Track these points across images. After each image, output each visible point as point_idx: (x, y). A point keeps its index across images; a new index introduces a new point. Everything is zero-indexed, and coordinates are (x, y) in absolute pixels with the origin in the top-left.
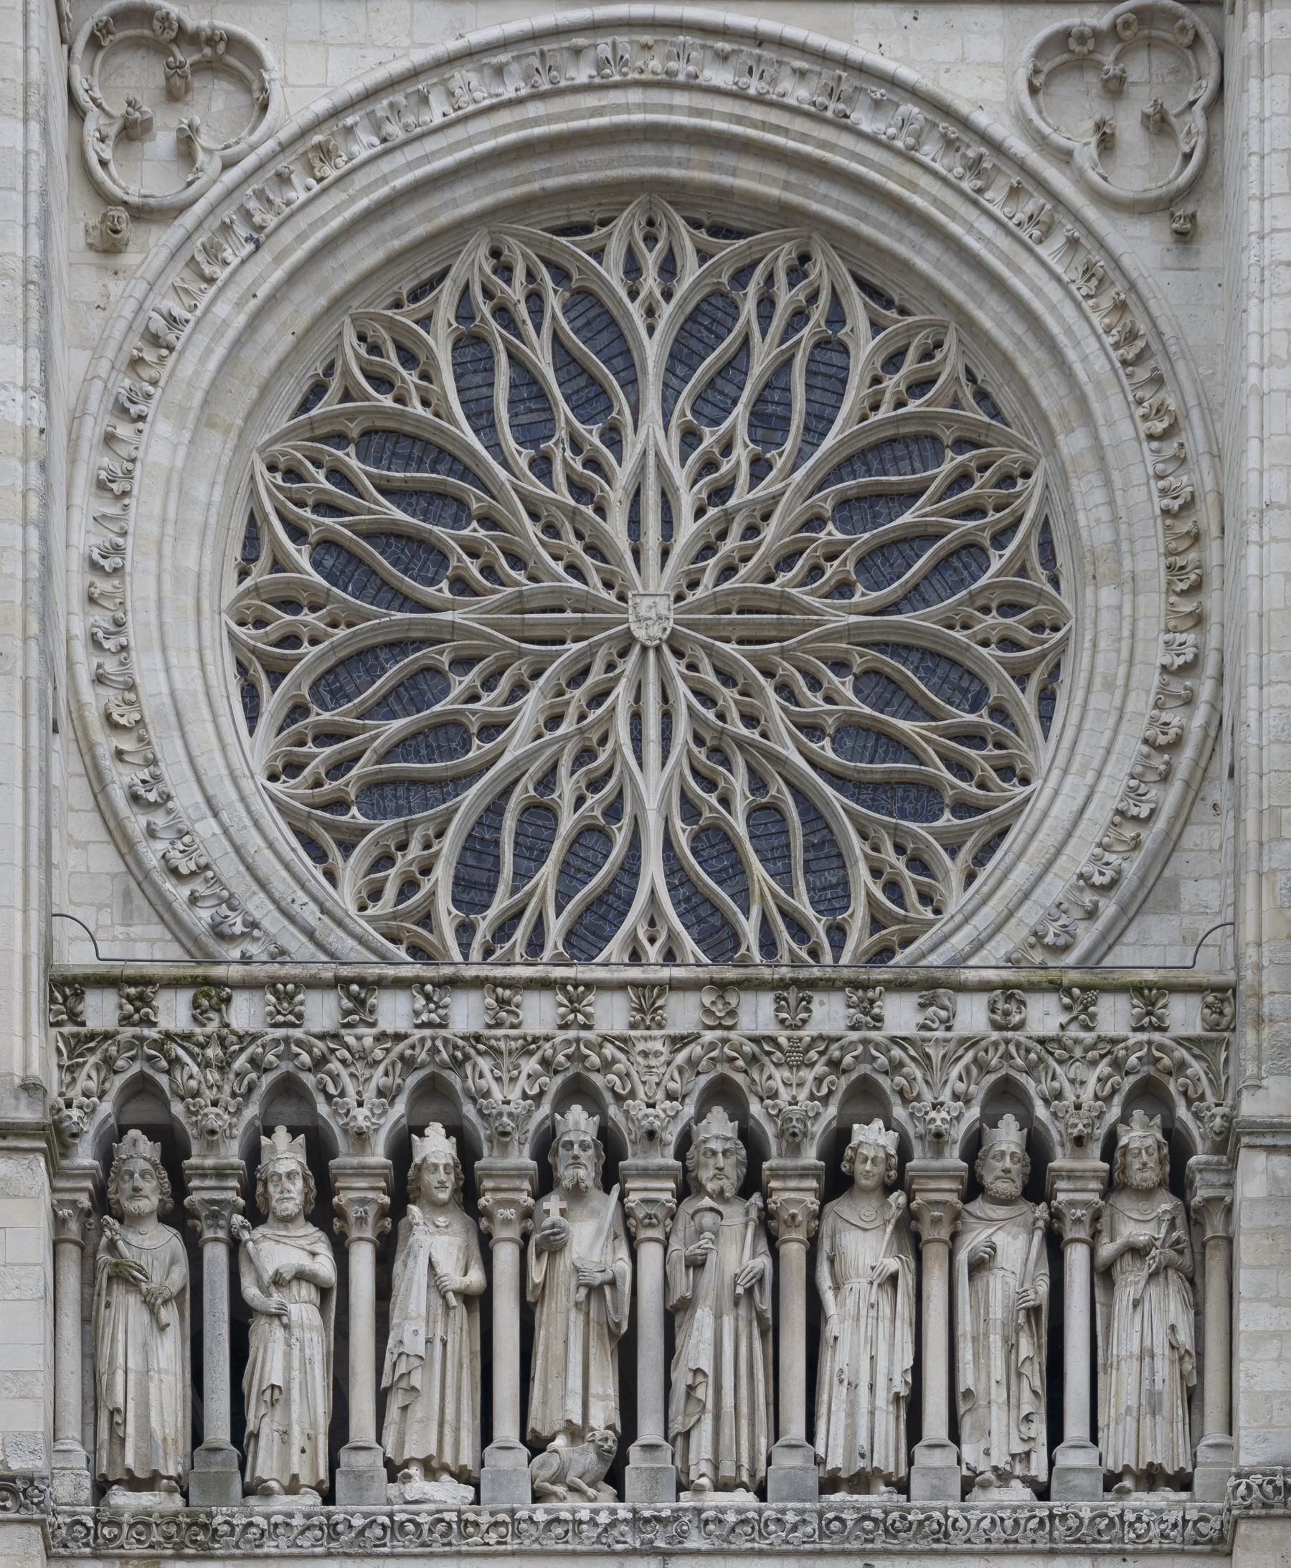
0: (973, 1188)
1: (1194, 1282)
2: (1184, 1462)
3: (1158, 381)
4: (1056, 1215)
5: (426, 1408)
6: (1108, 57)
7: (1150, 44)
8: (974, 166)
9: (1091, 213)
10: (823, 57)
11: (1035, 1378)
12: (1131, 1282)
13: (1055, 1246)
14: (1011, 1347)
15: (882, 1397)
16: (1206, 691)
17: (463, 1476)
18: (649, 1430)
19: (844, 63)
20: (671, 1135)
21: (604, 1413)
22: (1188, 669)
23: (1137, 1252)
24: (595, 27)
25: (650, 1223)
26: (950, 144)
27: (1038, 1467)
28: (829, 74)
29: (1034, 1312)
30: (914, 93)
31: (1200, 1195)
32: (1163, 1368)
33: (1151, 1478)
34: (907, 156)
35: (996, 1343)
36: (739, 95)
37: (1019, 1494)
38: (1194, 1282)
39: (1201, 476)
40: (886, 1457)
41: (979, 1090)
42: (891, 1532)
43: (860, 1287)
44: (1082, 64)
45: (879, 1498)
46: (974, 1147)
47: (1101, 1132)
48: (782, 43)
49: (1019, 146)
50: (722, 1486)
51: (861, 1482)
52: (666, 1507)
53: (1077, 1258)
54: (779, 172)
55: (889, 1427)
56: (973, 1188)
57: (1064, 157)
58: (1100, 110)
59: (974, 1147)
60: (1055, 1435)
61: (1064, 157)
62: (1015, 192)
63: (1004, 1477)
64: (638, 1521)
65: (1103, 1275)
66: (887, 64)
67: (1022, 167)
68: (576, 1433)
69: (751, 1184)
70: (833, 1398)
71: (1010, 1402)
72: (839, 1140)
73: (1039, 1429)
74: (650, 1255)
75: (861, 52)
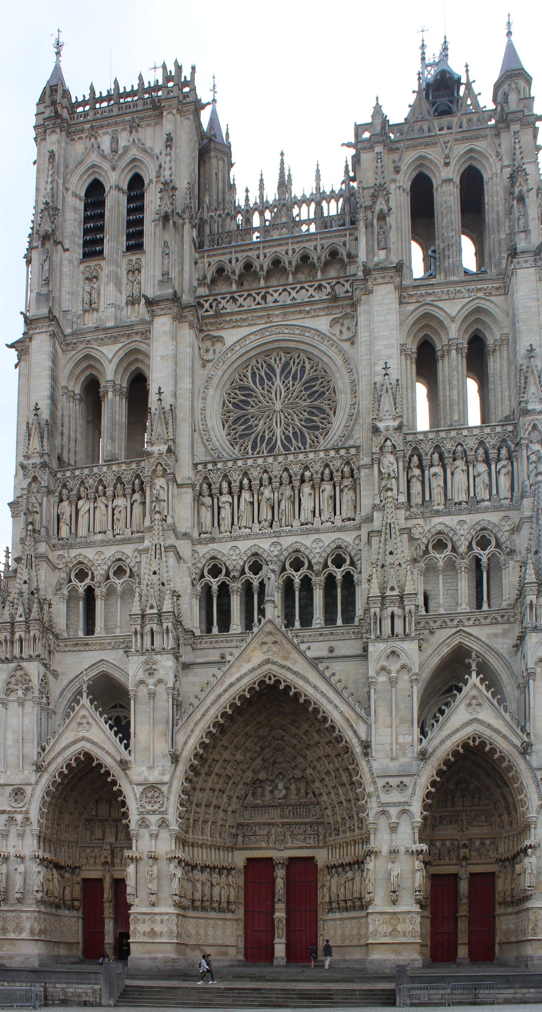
0: (322, 480)
1: (355, 490)
2: (353, 517)
3: (349, 364)
4: (334, 482)
5: (245, 518)
6: (341, 321)
7: (347, 318)
8: (322, 338)
9: (339, 342)
10: (301, 326)
11: (332, 506)
12: (346, 491)
13: (334, 487)
14: (328, 502)
15: (309, 511)
16: (357, 407)
17: (250, 528)
18: (276, 519)
19: (304, 327)
20: (279, 476)
21: (270, 517)
22: (354, 404)
23: (346, 486)
24: (269, 327)
25: (276, 489)
26: (319, 336)
27: (332, 520)
28: (301, 329)
29: (331, 497)
30: (313, 329)
31: (355, 477)
32: (350, 503)
33: (349, 519)
34: (313, 338)
35: (326, 502)
36: (289, 333)
37: (330, 523)
38: (355, 490)
39: (355, 377)
40: (310, 520)
41: (323, 465)
42: (311, 530)
43: (306, 495)
44: (337, 322)
45: (309, 526)
46: (322, 474)
47: (340, 469)
48: (295, 325)
49: (328, 334)
50: (287, 526)
51: (307, 524)
52: (278, 530)
53: (338, 488)
54: (295, 343)
55: (310, 515)
56: (322, 480)
57: (335, 335)
58: (340, 328)
59: (322, 474)
60: (335, 514)
61: (335, 335)
62: (328, 341)
63: (327, 521)
64: (274, 532)
65: (341, 491)
66: (310, 326)
67: (329, 337)
68: (266, 520)
69: (291, 482)
70: (302, 512)
71: (328, 510)
72: (303, 475)
73: (333, 514)
74: (276, 494)
75: (306, 325)
